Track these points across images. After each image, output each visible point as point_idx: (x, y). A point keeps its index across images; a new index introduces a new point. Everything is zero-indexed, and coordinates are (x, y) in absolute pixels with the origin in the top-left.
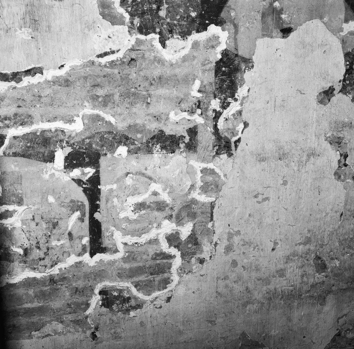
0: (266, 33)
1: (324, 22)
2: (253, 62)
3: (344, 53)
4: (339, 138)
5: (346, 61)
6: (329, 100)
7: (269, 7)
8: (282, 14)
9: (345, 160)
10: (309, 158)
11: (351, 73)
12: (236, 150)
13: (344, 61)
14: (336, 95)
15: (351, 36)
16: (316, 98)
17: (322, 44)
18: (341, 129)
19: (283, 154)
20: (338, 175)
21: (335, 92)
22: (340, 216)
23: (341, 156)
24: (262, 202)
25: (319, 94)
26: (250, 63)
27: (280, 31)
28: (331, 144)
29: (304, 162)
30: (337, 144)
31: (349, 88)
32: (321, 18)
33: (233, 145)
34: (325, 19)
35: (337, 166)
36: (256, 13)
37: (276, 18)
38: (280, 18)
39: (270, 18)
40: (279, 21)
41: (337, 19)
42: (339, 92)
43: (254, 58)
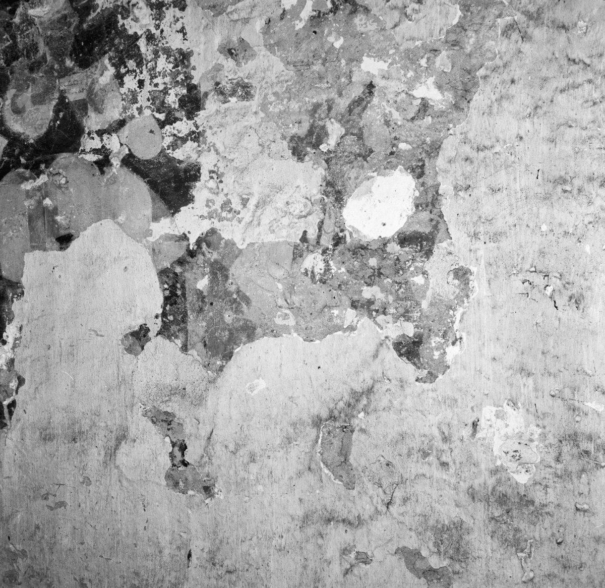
0: (36, 244)
1: (118, 224)
2: (22, 287)
3: (157, 270)
4: (166, 413)
5: (162, 283)
6: (143, 349)
7: (37, 207)
8: (57, 214)
9: (183, 455)
10: (120, 443)
11: (175, 303)
12: (10, 419)
13: (158, 284)
14: (152, 340)
15: (166, 243)
16: (120, 343)
17: (118, 257)
18: (167, 398)
19: (80, 433)
20: (173, 481)
22: (187, 557)
23: (173, 446)
24: (56, 508)
26: (18, 288)
27: (56, 239)
28: (153, 422)
29: (113, 451)
30: (165, 425)
31: (174, 328)
32: (114, 216)
33: (6, 411)
34: (120, 218)
35: (169, 464)
36: (21, 216)
37: (49, 222)
38: (55, 222)
39: (40, 223)
40: (52, 226)
41: (140, 216)
42: (157, 335)
43: (24, 280)
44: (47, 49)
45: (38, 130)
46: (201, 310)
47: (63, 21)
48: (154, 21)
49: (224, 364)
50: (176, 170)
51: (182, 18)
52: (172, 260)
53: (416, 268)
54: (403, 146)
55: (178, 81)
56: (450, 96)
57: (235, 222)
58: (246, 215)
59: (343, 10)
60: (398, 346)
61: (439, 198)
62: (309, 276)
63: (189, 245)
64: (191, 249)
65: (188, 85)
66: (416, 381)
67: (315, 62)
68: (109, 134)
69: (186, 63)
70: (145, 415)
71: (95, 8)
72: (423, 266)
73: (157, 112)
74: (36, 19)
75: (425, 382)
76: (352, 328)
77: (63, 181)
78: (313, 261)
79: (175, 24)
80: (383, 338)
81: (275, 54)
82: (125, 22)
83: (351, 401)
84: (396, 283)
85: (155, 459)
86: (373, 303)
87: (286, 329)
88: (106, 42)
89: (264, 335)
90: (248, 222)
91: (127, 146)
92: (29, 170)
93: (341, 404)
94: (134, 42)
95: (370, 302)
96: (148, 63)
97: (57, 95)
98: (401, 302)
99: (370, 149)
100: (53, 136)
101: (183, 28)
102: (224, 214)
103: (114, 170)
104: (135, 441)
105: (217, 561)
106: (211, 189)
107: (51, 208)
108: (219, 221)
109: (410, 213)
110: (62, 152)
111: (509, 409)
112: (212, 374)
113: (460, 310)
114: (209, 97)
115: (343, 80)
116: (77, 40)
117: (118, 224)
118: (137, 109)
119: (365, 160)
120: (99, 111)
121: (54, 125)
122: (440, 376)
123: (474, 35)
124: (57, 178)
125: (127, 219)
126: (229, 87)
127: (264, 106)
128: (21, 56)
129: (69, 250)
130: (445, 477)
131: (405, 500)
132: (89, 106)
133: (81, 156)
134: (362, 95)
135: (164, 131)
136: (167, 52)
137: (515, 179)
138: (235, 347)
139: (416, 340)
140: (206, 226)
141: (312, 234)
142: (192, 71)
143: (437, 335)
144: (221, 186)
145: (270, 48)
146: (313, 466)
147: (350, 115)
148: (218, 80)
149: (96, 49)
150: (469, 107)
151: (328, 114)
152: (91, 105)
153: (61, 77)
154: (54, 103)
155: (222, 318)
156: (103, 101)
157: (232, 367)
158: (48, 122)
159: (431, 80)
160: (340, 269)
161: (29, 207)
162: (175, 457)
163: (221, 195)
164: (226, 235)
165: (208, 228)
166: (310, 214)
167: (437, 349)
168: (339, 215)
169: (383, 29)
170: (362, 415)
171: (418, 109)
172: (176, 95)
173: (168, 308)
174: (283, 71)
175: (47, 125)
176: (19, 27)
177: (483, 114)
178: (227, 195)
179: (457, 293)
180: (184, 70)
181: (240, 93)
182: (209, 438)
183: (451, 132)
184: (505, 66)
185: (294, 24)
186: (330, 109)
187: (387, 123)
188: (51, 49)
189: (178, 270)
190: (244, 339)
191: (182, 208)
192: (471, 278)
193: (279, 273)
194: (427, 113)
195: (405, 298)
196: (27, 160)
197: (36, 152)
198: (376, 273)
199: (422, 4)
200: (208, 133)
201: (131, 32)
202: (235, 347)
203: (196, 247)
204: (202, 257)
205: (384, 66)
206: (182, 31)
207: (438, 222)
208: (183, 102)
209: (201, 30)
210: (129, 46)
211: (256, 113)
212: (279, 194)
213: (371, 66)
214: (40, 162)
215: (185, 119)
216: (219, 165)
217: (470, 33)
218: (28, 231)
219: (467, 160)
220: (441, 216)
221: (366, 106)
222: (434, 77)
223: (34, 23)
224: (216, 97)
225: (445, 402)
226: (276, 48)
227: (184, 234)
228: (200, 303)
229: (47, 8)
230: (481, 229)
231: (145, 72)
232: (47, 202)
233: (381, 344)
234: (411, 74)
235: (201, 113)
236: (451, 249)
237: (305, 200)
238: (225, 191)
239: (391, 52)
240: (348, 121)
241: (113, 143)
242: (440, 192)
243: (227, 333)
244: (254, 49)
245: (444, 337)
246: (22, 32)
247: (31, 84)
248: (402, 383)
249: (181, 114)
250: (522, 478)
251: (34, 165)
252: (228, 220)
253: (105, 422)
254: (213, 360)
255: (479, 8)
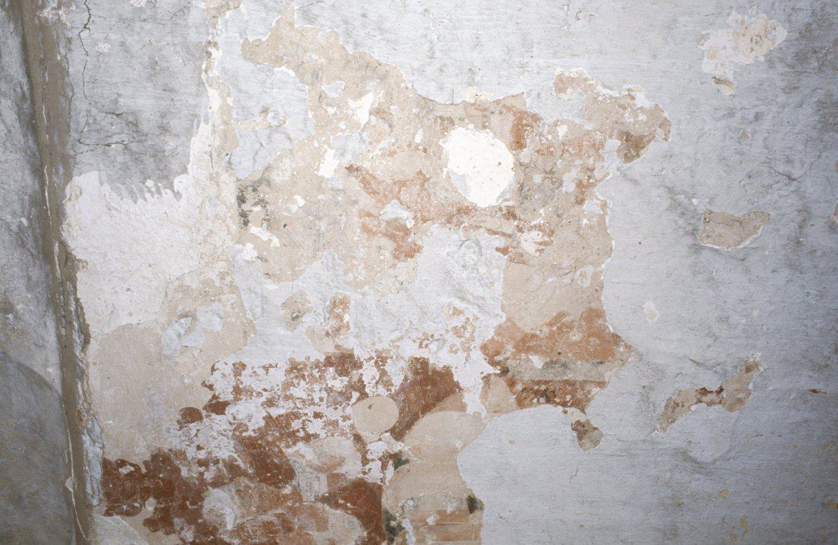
4: (666, 407)
5: (531, 405)
6: (596, 429)
8: (445, 511)
9: (711, 392)
13: (532, 409)
15: (489, 398)
16: (587, 452)
18: (651, 405)
19: (673, 499)
21: (583, 419)
25: (582, 447)
27: (471, 513)
29: (697, 465)
30: (678, 409)
31: (579, 395)
32: (455, 451)
35: (720, 406)
38: (452, 514)
39: (453, 530)
42: (584, 413)
44: (270, 512)
45: (354, 527)
46: (564, 365)
47: (243, 494)
48: (253, 398)
49: (624, 344)
50: (413, 384)
51: (253, 368)
52: (509, 393)
53: (549, 132)
54: (418, 139)
55: (320, 376)
56: (371, 83)
57: (477, 324)
58: (472, 311)
59: (265, 194)
60: (628, 158)
61: (478, 103)
62: (544, 247)
63: (495, 374)
64: (499, 372)
65: (325, 366)
66: (666, 140)
67: (317, 228)
68: (366, 452)
69: (302, 366)
70: (664, 429)
71: (232, 460)
72: (549, 125)
73: (350, 401)
74: (238, 521)
75: (669, 132)
76: (604, 206)
77: (411, 503)
78: (529, 242)
79: (259, 376)
80: (619, 173)
81: (304, 270)
82: (251, 428)
83: (678, 211)
84: (562, 155)
85: (712, 422)
86: (580, 182)
87: (596, 275)
88: (269, 449)
89: (599, 299)
90: (478, 310)
91: (382, 434)
92: (395, 538)
93: (681, 222)
94: (274, 421)
95: (580, 184)
96: (297, 407)
97: (319, 505)
98: (583, 152)
99: (418, 174)
100: (362, 511)
101: (264, 367)
102: (467, 335)
103: (406, 449)
104: (690, 442)
105: (823, 363)
106: (439, 349)
107: (438, 517)
108: (474, 340)
109: (491, 134)
110: (380, 502)
111: (706, 46)
112: (633, 357)
113: (600, 88)
114: (341, 344)
115: (340, 198)
116: (265, 480)
117: (465, 446)
118: (344, 421)
119: (429, 179)
120: (341, 462)
121: (350, 509)
122: (666, 115)
123: (308, 54)
124: (406, 510)
125: (459, 438)
126: (333, 322)
127: (357, 285)
128: (275, 540)
129: (484, 501)
130: (770, 117)
131: (789, 161)
132: (335, 472)
133: (387, 484)
134: (359, 179)
135: (370, 394)
136: (287, 385)
137: (467, 20)
138: (607, 331)
139: (625, 138)
140: (477, 355)
141: (500, 242)
142: (311, 360)
143: (622, 116)
144: (436, 337)
145: (295, 275)
146: (741, 256)
147: (379, 193)
148: (324, 333)
149: (276, 461)
150: (386, 65)
151: (375, 217)
152: (335, 470)
153: (301, 500)
154: (327, 508)
155: (576, 343)
156: (332, 456)
157: (629, 335)
158: (347, 516)
159: (351, 103)
160: (541, 214)
161: (433, 540)
162: (712, 400)
163: (447, 336)
164: (490, 334)
165: (479, 352)
166: (479, 243)
167: (637, 116)
168: (483, 212)
169: (291, 151)
170: (695, 201)
171: (380, 120)
172: (335, 379)
173: (557, 400)
174: (322, 263)
175: (350, 516)
176: (244, 540)
177: (395, 49)
178: (447, 331)
179: (580, 90)
180: (308, 369)
181: (340, 310)
182: (698, 364)
183: (410, 86)
184: (346, 23)
185: (273, 247)
186: (369, 215)
187: (392, 154)
188: (271, 508)
189: (519, 387)
190: (600, 322)
191: (455, 380)
192: (567, 74)
193: (537, 279)
194: (387, 110)
195: (579, 146)
196: (384, 539)
197: (377, 529)
198: (550, 176)
199: (269, 108)
200: (379, 347)
201: (262, 423)
202: (607, 331)
203: (498, 366)
204: (510, 360)
205: (331, 152)
206: (266, 368)
207: (504, 107)
208: (343, 372)
209: (269, 348)
210: (276, 426)
211: (363, 295)
212: (454, 276)
213: (329, 167)
214: (388, 525)
215: (360, 371)
216: (414, 338)
217: (306, 58)
218: (459, 541)
219: (441, 70)
220: (498, 102)
221: (371, 175)
222: (349, 100)
223: (241, 525)
224: (342, 337)
225: (693, 112)
226: (297, 269)
227: (483, 379)
228: (557, 366)
229: (227, 511)
230: (517, 60)
231: (306, 411)
232: (431, 520)
233: (625, 175)
234: (342, 125)
235: (356, 353)
236: (534, 94)
237: (463, 248)
238: (443, 332)
239: (316, 145)
240: (385, 196)
241: (377, 448)
242: (472, 101)
243: (592, 339)
244: (294, 292)
245: (625, 108)
246: (250, 537)
247: (305, 531)
248: (669, 156)
249: (355, 374)
250: (781, 35)
251: (391, 532)
252: (474, 331)
253: (666, 471)
254: (618, 356)
255: (281, 46)
